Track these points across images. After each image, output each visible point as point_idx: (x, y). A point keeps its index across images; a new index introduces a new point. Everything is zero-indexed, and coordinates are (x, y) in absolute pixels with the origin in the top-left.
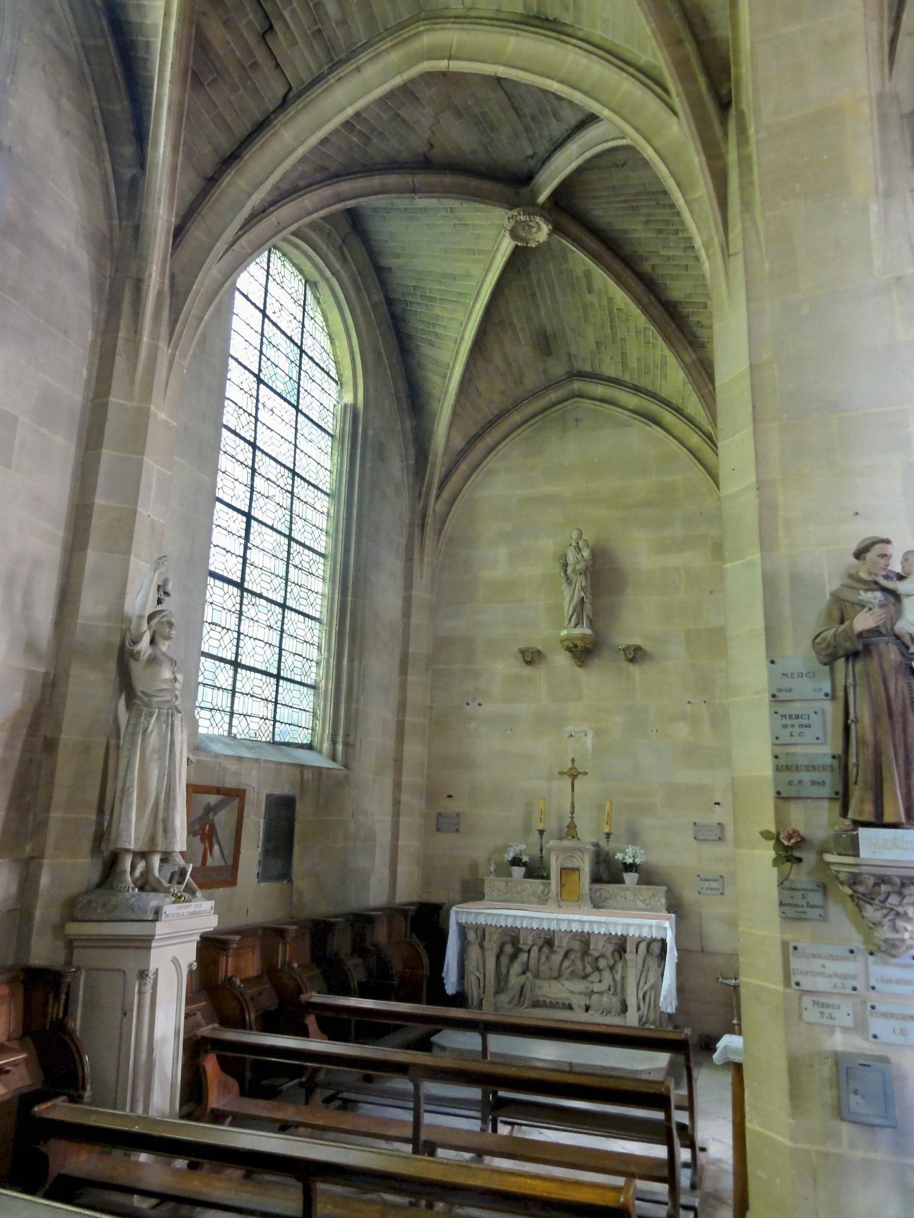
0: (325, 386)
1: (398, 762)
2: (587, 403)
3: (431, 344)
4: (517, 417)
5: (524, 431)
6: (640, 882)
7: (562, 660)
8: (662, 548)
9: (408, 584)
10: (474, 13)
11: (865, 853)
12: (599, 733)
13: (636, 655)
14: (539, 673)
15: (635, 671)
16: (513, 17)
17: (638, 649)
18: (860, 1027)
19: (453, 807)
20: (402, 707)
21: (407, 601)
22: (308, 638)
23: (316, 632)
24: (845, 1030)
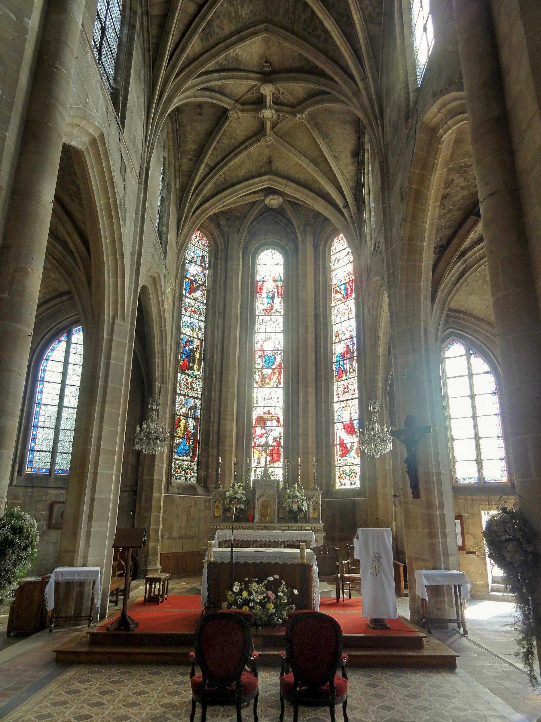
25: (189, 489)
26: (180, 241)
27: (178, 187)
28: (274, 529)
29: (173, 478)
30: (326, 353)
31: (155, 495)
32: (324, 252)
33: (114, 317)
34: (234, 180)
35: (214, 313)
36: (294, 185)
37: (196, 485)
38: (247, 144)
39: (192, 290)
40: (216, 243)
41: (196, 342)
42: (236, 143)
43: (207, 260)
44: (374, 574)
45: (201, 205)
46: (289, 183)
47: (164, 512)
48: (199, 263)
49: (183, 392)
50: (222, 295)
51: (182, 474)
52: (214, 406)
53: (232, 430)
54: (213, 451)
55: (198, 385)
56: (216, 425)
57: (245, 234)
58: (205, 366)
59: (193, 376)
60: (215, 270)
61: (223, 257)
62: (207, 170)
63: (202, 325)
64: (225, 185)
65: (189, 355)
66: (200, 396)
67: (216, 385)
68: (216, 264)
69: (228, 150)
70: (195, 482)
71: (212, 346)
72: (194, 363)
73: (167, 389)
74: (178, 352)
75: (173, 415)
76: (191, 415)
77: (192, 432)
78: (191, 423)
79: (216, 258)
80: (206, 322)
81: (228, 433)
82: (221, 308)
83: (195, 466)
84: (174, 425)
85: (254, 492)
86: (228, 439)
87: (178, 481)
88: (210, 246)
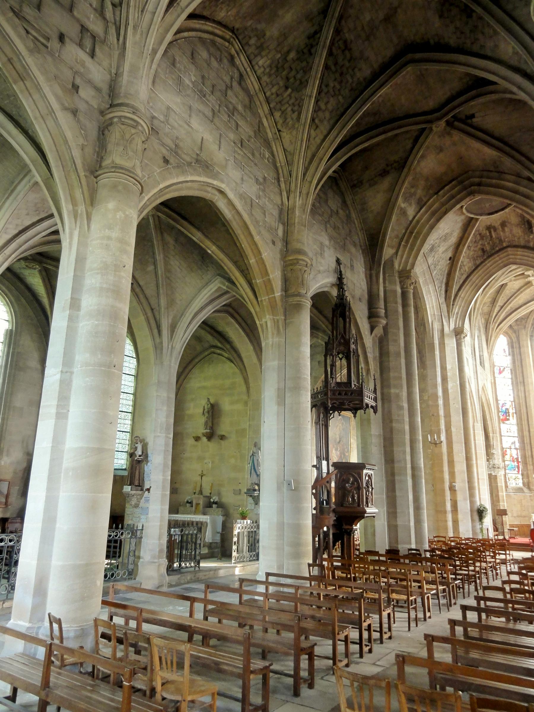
0: (131, 362)
2: (215, 355)
4: (197, 360)
5: (199, 365)
6: (217, 507)
7: (204, 439)
8: (232, 403)
12: (213, 462)
13: (222, 437)
14: (199, 444)
15: (222, 442)
17: (224, 436)
18: (132, 520)
19: (177, 486)
22: (124, 438)
23: (128, 436)
25: (519, 490)
26: (490, 351)
27: (483, 322)
29: (508, 484)
31: (500, 494)
33: (474, 422)
34: (517, 307)
35: (517, 383)
38: (521, 290)
39: (500, 373)
40: (510, 338)
42: (515, 291)
45: (499, 325)
47: (507, 502)
57: (529, 328)
58: (517, 417)
60: (513, 356)
61: (517, 346)
62: (499, 308)
64: (512, 311)
65: (506, 412)
66: (517, 436)
67: (525, 427)
68: (513, 352)
69: (510, 295)
71: (519, 403)
72: (509, 416)
73: (497, 436)
74: (499, 412)
75: (502, 448)
77: (515, 457)
83: (520, 476)
84: (504, 454)
87: (511, 485)
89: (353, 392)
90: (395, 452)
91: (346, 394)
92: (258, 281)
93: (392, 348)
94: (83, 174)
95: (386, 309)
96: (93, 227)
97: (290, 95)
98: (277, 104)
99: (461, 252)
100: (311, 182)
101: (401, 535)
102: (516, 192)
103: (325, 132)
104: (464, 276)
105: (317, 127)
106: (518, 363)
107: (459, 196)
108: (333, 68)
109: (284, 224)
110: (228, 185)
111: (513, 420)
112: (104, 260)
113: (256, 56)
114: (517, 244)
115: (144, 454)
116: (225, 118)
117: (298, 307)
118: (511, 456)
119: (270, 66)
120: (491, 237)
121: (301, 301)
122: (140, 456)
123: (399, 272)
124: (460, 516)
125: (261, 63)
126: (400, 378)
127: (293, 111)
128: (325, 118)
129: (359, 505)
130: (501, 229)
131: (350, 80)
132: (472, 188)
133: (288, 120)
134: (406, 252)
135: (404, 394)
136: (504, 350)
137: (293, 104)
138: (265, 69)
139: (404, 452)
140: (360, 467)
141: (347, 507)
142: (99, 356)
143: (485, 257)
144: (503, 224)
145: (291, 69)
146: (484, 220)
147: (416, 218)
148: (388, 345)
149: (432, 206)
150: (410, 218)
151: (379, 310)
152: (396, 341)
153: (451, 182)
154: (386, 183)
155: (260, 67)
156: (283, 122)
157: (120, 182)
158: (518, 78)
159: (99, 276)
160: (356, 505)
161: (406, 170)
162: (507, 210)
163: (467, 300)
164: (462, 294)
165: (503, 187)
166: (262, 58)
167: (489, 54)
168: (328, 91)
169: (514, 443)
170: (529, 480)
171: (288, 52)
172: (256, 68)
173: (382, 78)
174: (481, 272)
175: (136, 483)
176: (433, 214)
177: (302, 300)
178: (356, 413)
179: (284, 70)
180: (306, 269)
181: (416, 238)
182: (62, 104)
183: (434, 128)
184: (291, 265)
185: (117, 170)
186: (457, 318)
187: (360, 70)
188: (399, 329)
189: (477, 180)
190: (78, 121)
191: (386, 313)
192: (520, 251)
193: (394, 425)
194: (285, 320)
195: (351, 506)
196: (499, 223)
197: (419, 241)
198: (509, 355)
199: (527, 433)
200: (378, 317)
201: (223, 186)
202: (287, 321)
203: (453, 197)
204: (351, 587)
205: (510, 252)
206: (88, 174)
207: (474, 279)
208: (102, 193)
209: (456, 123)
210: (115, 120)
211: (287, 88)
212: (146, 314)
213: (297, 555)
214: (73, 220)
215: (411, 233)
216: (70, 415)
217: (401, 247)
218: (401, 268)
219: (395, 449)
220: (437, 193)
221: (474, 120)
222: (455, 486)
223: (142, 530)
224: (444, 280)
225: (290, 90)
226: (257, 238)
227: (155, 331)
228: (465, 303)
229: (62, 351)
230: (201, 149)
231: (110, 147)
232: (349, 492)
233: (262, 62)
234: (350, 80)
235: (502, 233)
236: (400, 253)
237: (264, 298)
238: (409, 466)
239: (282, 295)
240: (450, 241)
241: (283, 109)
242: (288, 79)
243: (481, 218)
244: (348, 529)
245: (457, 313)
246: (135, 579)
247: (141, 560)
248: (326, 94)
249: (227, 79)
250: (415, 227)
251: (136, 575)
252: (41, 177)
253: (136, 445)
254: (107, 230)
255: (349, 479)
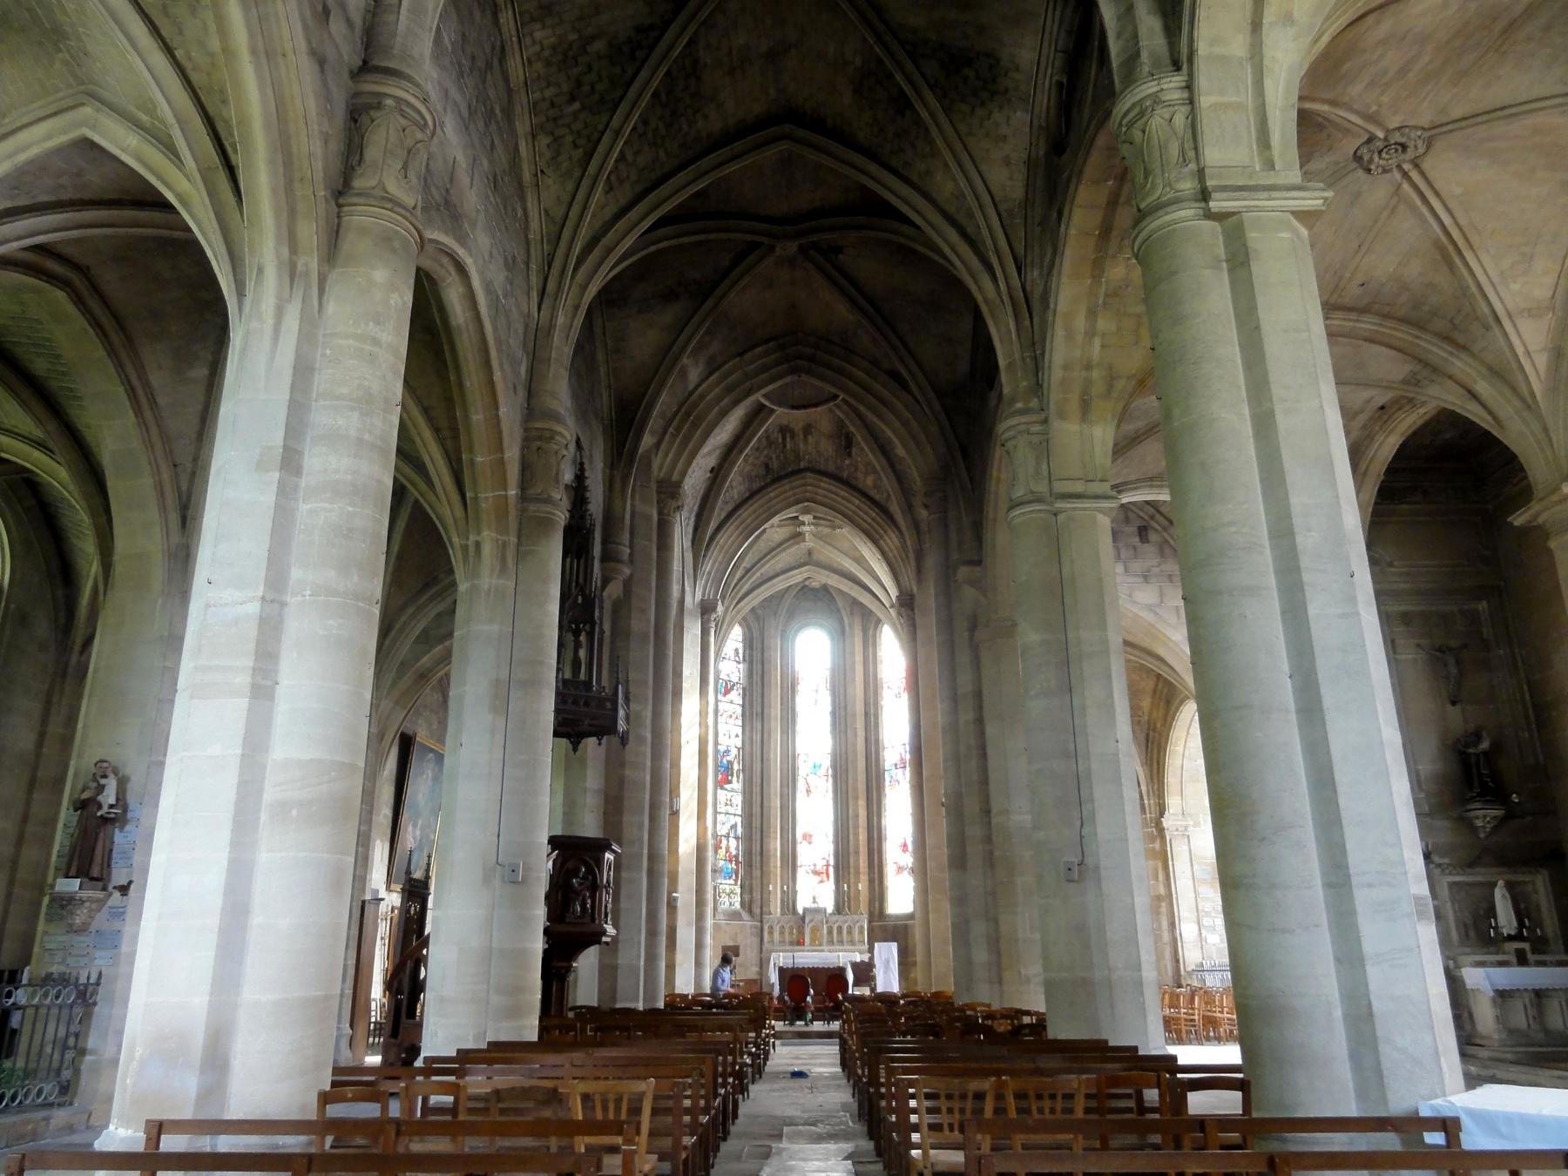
1: (14, 863)
3: (78, 537)
9: (45, 719)
10: (16, 430)
11: (57, 889)
16: (34, 438)
18: (63, 962)
20: (25, 819)
21: (42, 736)
24: (58, 963)
25: (734, 916)
28: (823, 951)
30: (877, 760)
32: (875, 637)
34: (772, 573)
36: (836, 576)
37: (741, 910)
39: (727, 692)
41: (734, 752)
42: (773, 545)
43: (741, 652)
44: (885, 972)
45: (737, 604)
46: (832, 574)
48: (732, 658)
49: (723, 810)
50: (760, 692)
51: (726, 899)
52: (756, 823)
53: (776, 850)
54: (757, 873)
55: (738, 799)
56: (759, 842)
59: (733, 790)
63: (739, 731)
65: (728, 768)
68: (751, 656)
70: (739, 907)
72: (732, 775)
76: (732, 835)
77: (734, 853)
78: (733, 843)
79: (751, 648)
80: (743, 726)
81: (772, 853)
82: (759, 710)
83: (738, 890)
84: (717, 847)
85: (803, 918)
86: (772, 860)
88: (744, 634)
89: (601, 702)
90: (624, 825)
91: (586, 704)
92: (479, 459)
93: (636, 625)
94: (323, 193)
95: (631, 547)
96: (331, 308)
97: (575, 114)
98: (548, 120)
99: (734, 463)
100: (584, 288)
101: (623, 983)
102: (868, 390)
103: (623, 202)
104: (730, 507)
105: (611, 189)
106: (757, 678)
107: (774, 371)
108: (664, 98)
109: (528, 354)
110: (475, 262)
111: (737, 784)
112: (366, 383)
113: (533, 20)
114: (822, 468)
115: (121, 803)
116: (481, 124)
117: (545, 524)
118: (727, 850)
119: (554, 48)
120: (785, 446)
121: (554, 514)
122: (111, 806)
123: (658, 482)
124: (679, 957)
125: (538, 35)
126: (646, 682)
127: (576, 146)
128: (628, 177)
129: (593, 920)
130: (801, 436)
131: (685, 127)
132: (799, 362)
133: (561, 158)
134: (673, 450)
135: (649, 714)
136: (737, 650)
137: (578, 133)
138: (543, 49)
139: (641, 827)
140: (601, 846)
141: (569, 923)
142: (356, 579)
143: (769, 480)
144: (807, 430)
145: (590, 68)
146: (781, 414)
147: (700, 389)
148: (629, 618)
149: (729, 373)
150: (691, 388)
151: (621, 547)
152: (643, 611)
153: (767, 341)
154: (668, 315)
155: (534, 42)
156: (554, 158)
157: (397, 232)
158: (953, 235)
159: (356, 415)
160: (587, 920)
161: (710, 302)
162: (819, 409)
163: (727, 552)
164: (722, 539)
165: (850, 377)
166: (544, 28)
167: (915, 178)
168: (645, 133)
169: (734, 827)
170: (752, 897)
171: (593, 38)
172: (528, 40)
173: (738, 146)
174: (756, 505)
175: (95, 872)
176: (729, 390)
177: (556, 512)
178: (579, 742)
179: (577, 64)
180: (565, 453)
181: (695, 426)
182: (309, 42)
183: (778, 249)
184: (540, 438)
185: (397, 209)
186: (707, 582)
187: (706, 117)
188: (650, 591)
189: (808, 351)
190: (325, 83)
191: (631, 555)
192: (825, 483)
193: (628, 772)
194: (519, 544)
195: (580, 921)
196: (801, 425)
197: (699, 432)
198: (744, 660)
199: (759, 809)
200: (619, 561)
201: (469, 262)
202: (522, 549)
203: (765, 369)
204: (729, 1028)
205: (809, 481)
206: (328, 196)
207: (744, 516)
208: (350, 243)
209: (812, 252)
210: (389, 102)
211: (572, 99)
212: (159, 473)
213: (515, 1012)
214: (287, 280)
215: (688, 414)
216: (281, 691)
217: (667, 436)
218: (661, 475)
219: (625, 819)
220: (741, 354)
221: (841, 256)
222: (675, 899)
223: (98, 984)
224: (696, 508)
225: (576, 106)
226: (497, 376)
227: (174, 518)
228: (724, 557)
229: (263, 553)
230: (451, 180)
231: (372, 153)
232: (577, 893)
233: (542, 35)
234: (685, 127)
235: (802, 445)
236: (663, 446)
237: (486, 497)
238: (646, 851)
239: (517, 494)
240: (718, 438)
241: (558, 132)
242: (579, 84)
243: (780, 410)
244: (562, 968)
245: (710, 573)
246: (71, 1104)
247: (88, 1058)
248: (640, 136)
249: (488, 49)
250: (695, 405)
251: (75, 1094)
252: (196, 160)
253: (103, 781)
254: (371, 324)
255: (580, 870)
